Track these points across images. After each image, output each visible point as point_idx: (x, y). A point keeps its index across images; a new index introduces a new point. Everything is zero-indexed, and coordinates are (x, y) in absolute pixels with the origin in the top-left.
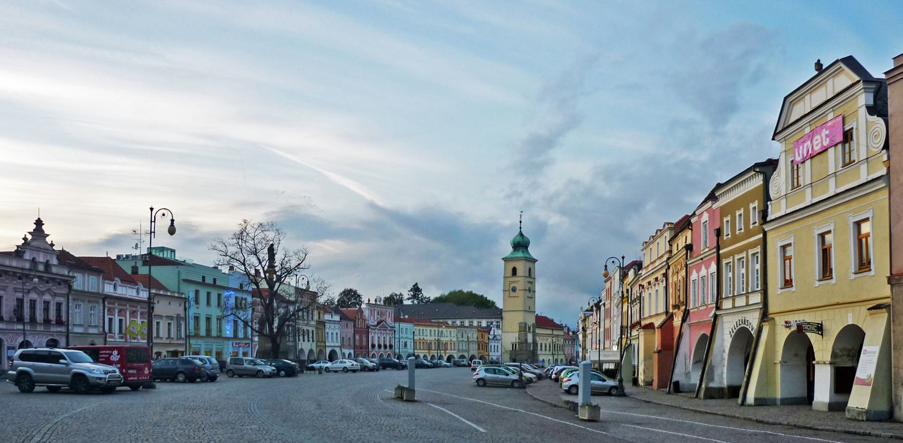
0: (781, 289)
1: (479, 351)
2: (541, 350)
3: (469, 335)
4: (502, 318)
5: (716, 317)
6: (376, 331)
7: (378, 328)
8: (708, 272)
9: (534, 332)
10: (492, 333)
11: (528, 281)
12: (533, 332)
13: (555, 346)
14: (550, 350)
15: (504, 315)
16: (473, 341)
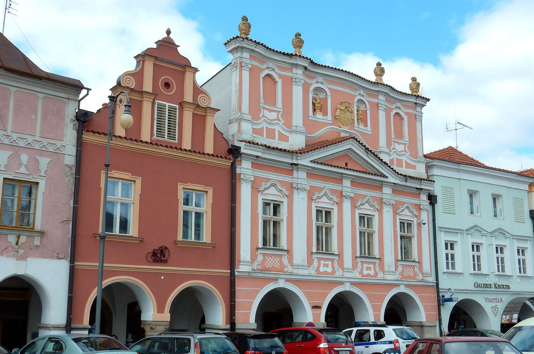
6: (300, 177)
7: (305, 161)
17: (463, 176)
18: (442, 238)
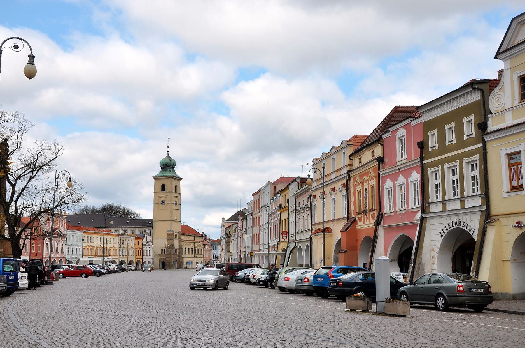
0: (508, 193)
1: (136, 257)
2: (185, 253)
3: (128, 242)
5: (422, 219)
8: (407, 181)
9: (179, 238)
10: (145, 239)
13: (196, 251)
14: (192, 254)
15: (154, 224)
16: (132, 247)
17: (72, 232)
18: (67, 247)
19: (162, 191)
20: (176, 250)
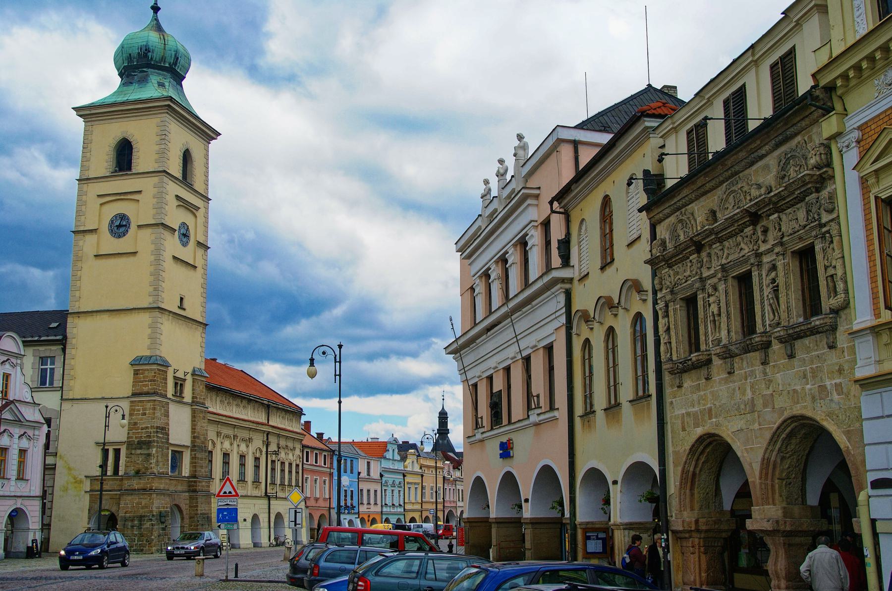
4: (63, 343)
11: (178, 197)
12: (194, 402)
15: (77, 329)
19: (116, 171)
20: (177, 457)
